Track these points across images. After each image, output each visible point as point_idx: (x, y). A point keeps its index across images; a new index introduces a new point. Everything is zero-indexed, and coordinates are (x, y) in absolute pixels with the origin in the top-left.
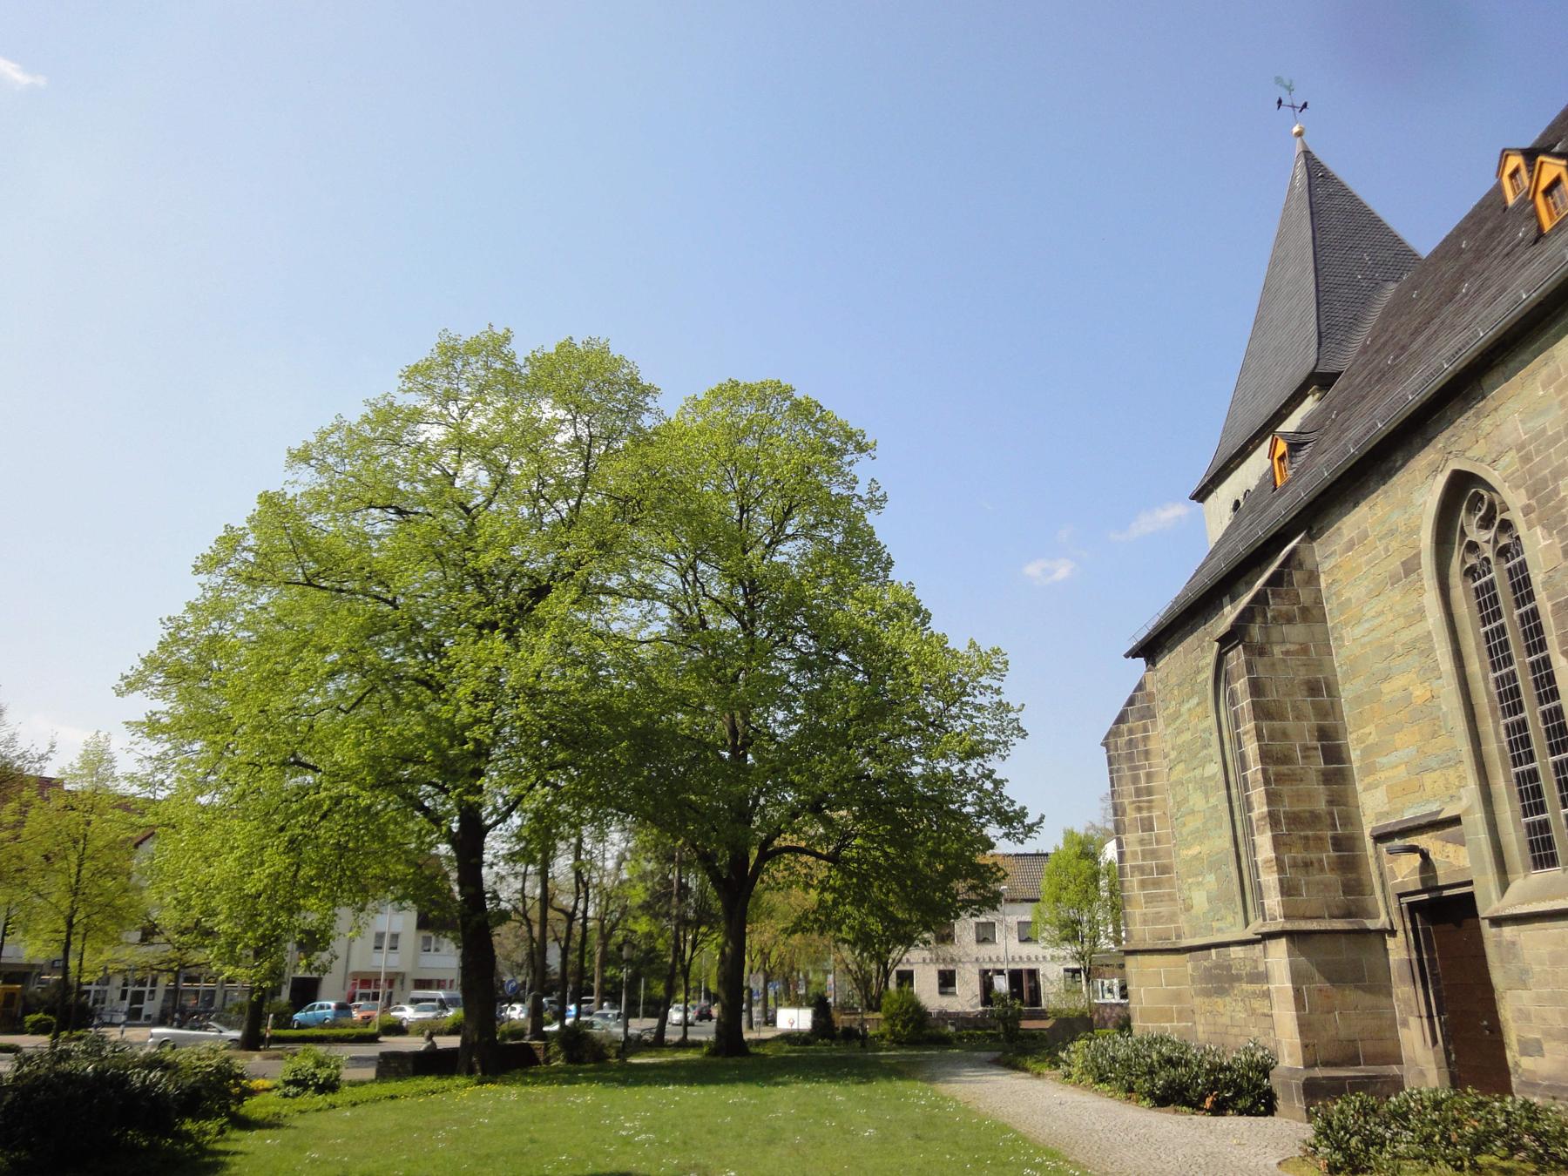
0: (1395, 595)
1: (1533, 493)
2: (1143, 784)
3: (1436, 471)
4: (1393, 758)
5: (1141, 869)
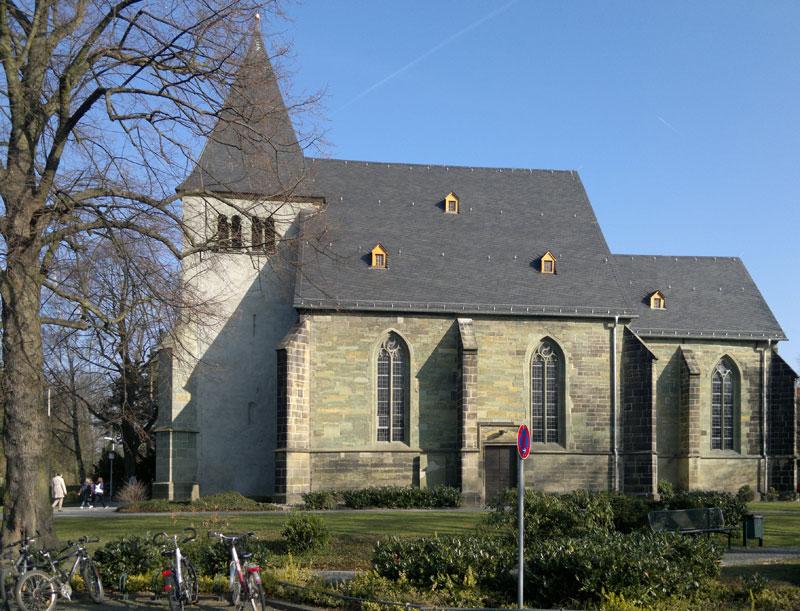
0: (510, 358)
1: (573, 355)
2: (300, 374)
3: (540, 331)
4: (494, 403)
5: (296, 413)
